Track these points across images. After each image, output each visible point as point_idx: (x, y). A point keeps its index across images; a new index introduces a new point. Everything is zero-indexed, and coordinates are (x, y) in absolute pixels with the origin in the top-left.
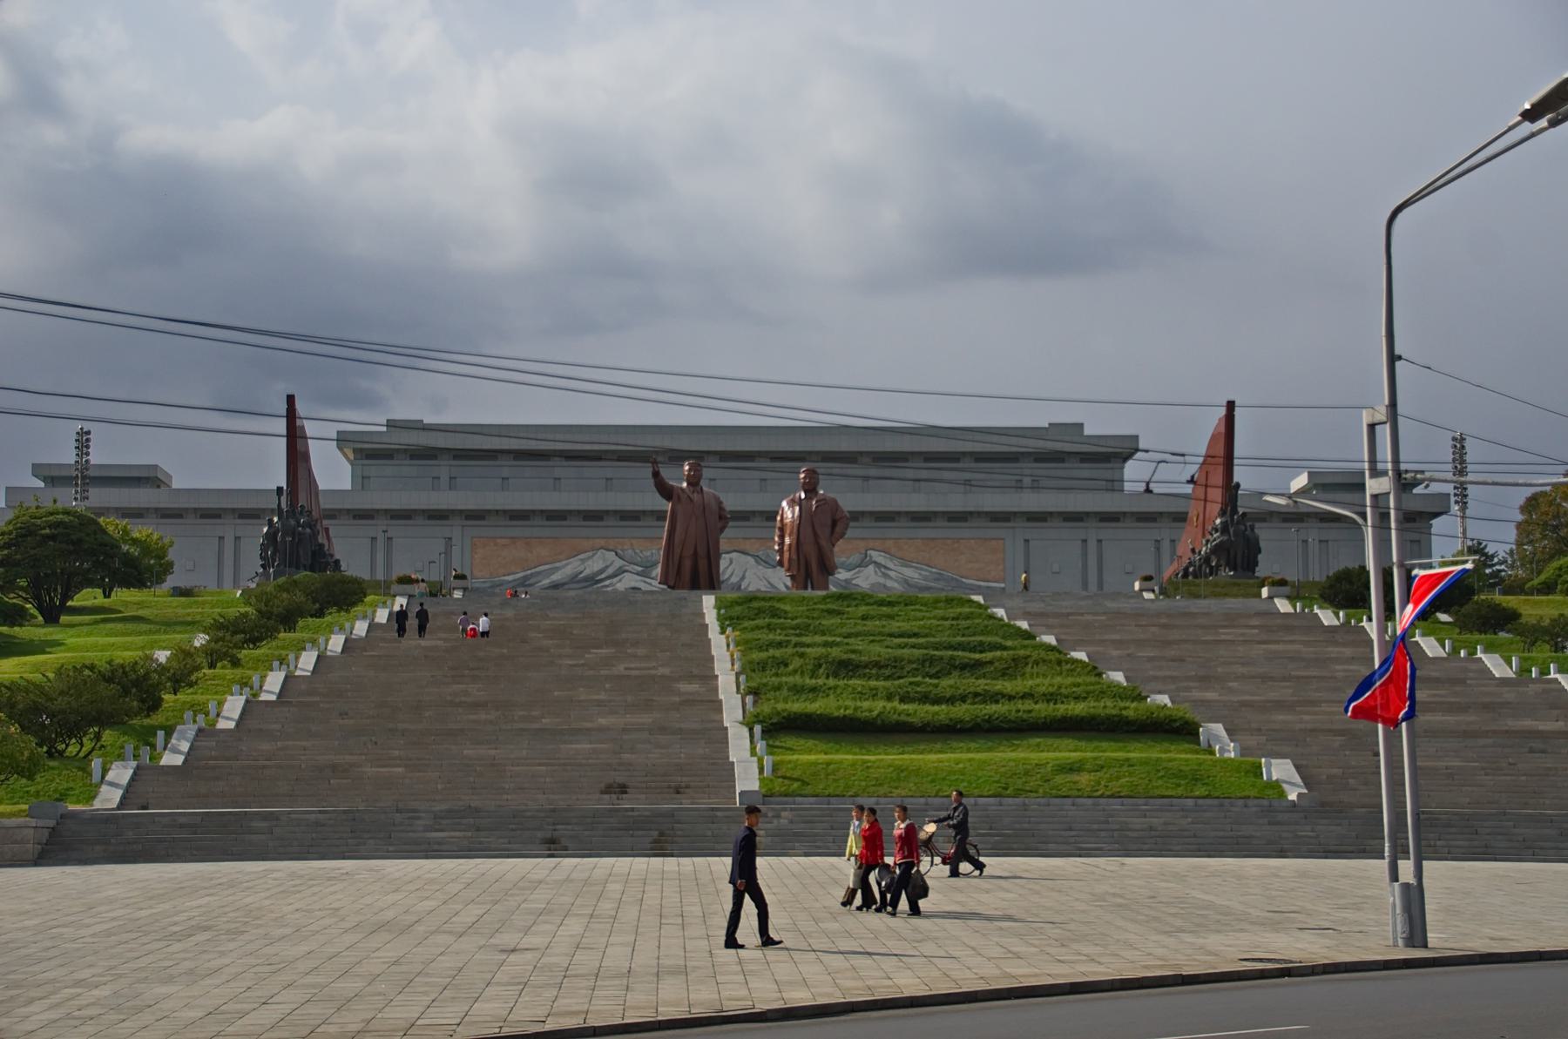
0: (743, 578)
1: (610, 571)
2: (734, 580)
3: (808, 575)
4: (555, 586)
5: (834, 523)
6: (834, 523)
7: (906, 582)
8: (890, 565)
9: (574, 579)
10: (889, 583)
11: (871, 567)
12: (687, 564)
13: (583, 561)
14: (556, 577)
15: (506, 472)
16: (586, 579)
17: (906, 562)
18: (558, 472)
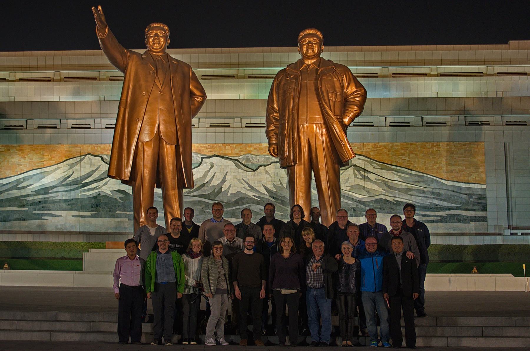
1: (96, 175)
4: (46, 190)
8: (370, 169)
10: (369, 186)
11: (351, 170)
14: (48, 181)
16: (75, 182)
17: (384, 165)
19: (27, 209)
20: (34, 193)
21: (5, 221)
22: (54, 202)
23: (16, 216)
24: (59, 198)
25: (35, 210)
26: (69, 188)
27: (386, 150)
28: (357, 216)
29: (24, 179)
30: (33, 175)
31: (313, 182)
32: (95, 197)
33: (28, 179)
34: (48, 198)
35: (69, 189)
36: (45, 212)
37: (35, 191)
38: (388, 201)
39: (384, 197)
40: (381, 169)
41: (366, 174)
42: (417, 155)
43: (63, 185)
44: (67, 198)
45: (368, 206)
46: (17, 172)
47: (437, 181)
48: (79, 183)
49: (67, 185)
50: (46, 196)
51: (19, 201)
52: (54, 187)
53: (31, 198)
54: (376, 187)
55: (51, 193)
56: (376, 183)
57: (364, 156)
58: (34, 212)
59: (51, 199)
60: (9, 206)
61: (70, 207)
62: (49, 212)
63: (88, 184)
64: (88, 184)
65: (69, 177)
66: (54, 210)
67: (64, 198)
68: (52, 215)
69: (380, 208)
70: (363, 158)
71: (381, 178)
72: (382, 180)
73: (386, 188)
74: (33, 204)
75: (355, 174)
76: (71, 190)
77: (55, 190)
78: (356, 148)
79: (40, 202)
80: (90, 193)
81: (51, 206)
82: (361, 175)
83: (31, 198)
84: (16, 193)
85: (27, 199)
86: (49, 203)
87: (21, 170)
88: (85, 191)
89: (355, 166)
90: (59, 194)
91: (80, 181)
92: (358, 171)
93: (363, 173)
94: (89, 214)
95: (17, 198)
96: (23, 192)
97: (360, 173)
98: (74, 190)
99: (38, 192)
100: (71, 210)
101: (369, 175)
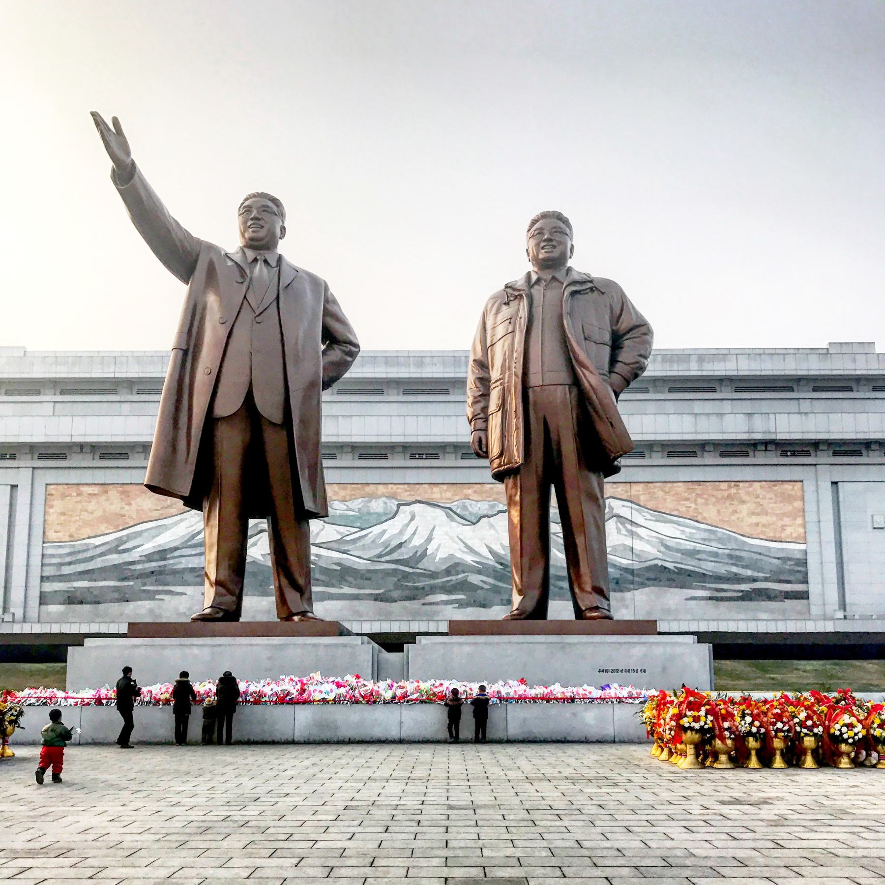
0: (429, 540)
2: (417, 541)
4: (162, 554)
10: (639, 546)
14: (165, 539)
19: (132, 583)
20: (143, 558)
21: (98, 603)
22: (175, 572)
23: (116, 595)
24: (182, 566)
25: (145, 585)
27: (660, 494)
28: (622, 591)
29: (129, 538)
31: (554, 510)
33: (135, 538)
34: (165, 566)
35: (198, 552)
36: (161, 588)
37: (145, 556)
38: (666, 568)
39: (660, 563)
40: (656, 521)
41: (634, 529)
42: (707, 500)
44: (195, 566)
45: (638, 576)
46: (118, 526)
47: (736, 539)
49: (195, 546)
50: (162, 563)
51: (121, 571)
52: (176, 549)
53: (139, 567)
55: (169, 559)
56: (648, 542)
57: (631, 502)
58: (144, 588)
59: (171, 567)
60: (105, 580)
61: (198, 579)
62: (167, 588)
66: (174, 585)
67: (190, 566)
69: (655, 579)
70: (629, 504)
71: (657, 535)
72: (657, 538)
73: (663, 549)
75: (617, 528)
77: (177, 553)
78: (620, 490)
79: (152, 572)
81: (169, 578)
82: (627, 530)
83: (139, 567)
84: (115, 559)
86: (167, 574)
87: (126, 523)
89: (618, 516)
90: (183, 560)
92: (623, 524)
93: (629, 527)
95: (115, 566)
97: (625, 527)
99: (149, 558)
101: (639, 530)
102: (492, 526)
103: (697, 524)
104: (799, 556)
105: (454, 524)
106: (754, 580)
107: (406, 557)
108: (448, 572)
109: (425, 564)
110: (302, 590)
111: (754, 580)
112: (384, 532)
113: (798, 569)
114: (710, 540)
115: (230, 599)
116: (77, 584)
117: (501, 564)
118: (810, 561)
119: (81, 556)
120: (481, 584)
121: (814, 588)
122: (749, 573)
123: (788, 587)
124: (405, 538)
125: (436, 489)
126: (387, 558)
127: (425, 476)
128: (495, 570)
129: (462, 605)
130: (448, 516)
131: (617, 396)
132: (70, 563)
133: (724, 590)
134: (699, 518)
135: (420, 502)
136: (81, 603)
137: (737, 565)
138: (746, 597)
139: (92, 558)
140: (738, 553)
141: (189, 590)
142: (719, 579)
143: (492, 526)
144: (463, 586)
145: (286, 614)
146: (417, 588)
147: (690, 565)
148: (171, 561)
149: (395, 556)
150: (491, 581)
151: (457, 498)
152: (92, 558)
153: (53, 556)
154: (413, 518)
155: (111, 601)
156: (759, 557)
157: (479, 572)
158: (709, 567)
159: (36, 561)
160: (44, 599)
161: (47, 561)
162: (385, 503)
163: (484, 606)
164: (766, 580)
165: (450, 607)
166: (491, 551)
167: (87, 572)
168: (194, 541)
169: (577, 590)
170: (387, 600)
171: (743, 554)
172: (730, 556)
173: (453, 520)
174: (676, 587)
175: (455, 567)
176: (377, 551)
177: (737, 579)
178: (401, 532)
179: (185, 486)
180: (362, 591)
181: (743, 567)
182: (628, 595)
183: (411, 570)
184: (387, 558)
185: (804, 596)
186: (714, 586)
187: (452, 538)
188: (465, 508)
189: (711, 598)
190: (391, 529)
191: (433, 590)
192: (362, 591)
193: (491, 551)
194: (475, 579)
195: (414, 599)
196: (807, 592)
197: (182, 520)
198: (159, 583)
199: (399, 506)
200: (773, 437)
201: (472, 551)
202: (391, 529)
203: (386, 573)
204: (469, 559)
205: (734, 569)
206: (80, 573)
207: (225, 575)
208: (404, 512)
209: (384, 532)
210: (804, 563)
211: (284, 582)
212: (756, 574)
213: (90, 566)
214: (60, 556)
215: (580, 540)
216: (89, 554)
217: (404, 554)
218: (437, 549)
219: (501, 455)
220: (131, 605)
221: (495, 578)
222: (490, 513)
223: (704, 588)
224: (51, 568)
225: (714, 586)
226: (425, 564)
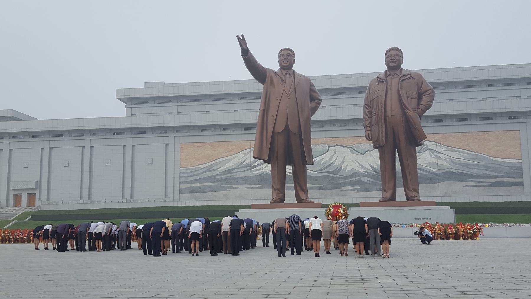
0: (343, 162)
2: (338, 163)
3: (396, 146)
4: (229, 171)
5: (420, 97)
6: (420, 97)
7: (452, 161)
8: (441, 151)
9: (239, 166)
10: (440, 162)
12: (280, 141)
13: (245, 155)
14: (229, 165)
15: (208, 108)
16: (247, 166)
17: (450, 147)
18: (236, 107)
21: (203, 192)
22: (234, 179)
24: (237, 176)
26: (244, 169)
27: (451, 138)
30: (220, 162)
32: (260, 175)
39: (451, 170)
43: (241, 168)
48: (251, 167)
49: (241, 168)
51: (212, 179)
52: (234, 169)
53: (219, 177)
54: (445, 163)
56: (445, 160)
61: (244, 182)
62: (231, 186)
63: (256, 166)
64: (256, 166)
65: (244, 162)
68: (233, 188)
73: (452, 163)
74: (220, 181)
75: (430, 154)
76: (245, 171)
77: (235, 171)
80: (257, 172)
83: (219, 177)
84: (210, 174)
85: (217, 177)
88: (254, 171)
89: (430, 149)
91: (250, 165)
92: (433, 153)
93: (436, 154)
94: (257, 186)
95: (210, 177)
96: (214, 173)
98: (247, 170)
99: (223, 173)
100: (245, 184)
101: (440, 155)
102: (371, 155)
103: (468, 152)
104: (518, 165)
105: (354, 155)
106: (497, 177)
107: (333, 170)
108: (352, 176)
109: (341, 173)
110: (305, 191)
111: (497, 177)
112: (323, 159)
113: (518, 171)
114: (475, 159)
115: (281, 195)
116: (194, 185)
117: (376, 172)
118: (523, 167)
119: (195, 173)
120: (367, 182)
121: (526, 180)
122: (494, 174)
123: (513, 180)
124: (332, 162)
125: (345, 139)
126: (324, 171)
127: (341, 134)
128: (373, 175)
129: (358, 191)
130: (351, 151)
131: (420, 117)
132: (191, 176)
133: (482, 182)
134: (469, 149)
135: (338, 145)
136: (196, 193)
137: (488, 170)
138: (493, 185)
139: (200, 174)
140: (488, 165)
141: (240, 186)
142: (479, 177)
143: (371, 155)
144: (359, 182)
145: (299, 200)
146: (338, 184)
147: (466, 171)
148: (232, 174)
149: (328, 170)
150: (371, 180)
151: (355, 143)
152: (200, 174)
153: (183, 173)
154: (335, 153)
155: (209, 192)
156: (498, 166)
157: (366, 176)
158: (475, 171)
159: (177, 176)
160: (181, 191)
161: (182, 175)
162: (323, 146)
163: (368, 191)
164: (502, 177)
165: (353, 192)
166: (372, 167)
167: (198, 179)
168: (241, 166)
169: (407, 190)
170: (325, 190)
171: (490, 165)
172: (485, 167)
173: (354, 153)
174: (459, 181)
175: (355, 174)
176: (320, 168)
177: (488, 177)
178: (331, 159)
179: (266, 158)
180: (314, 186)
181: (491, 171)
182: (436, 185)
183: (335, 176)
184: (324, 171)
185: (521, 184)
186: (477, 180)
187: (353, 161)
188: (359, 147)
189: (475, 186)
190: (326, 158)
191: (345, 184)
192: (314, 186)
193: (372, 167)
194: (364, 179)
195: (336, 188)
196: (523, 182)
197: (236, 157)
198: (227, 183)
199: (329, 147)
200: (504, 111)
201: (362, 167)
202: (326, 158)
203: (324, 177)
204: (361, 170)
205: (487, 172)
206: (196, 180)
207: (279, 187)
208: (331, 150)
209: (323, 159)
210: (521, 169)
211: (298, 188)
212: (497, 174)
213: (199, 177)
214: (187, 173)
215: (407, 171)
216: (199, 172)
217: (331, 169)
218: (347, 166)
219: (377, 141)
220: (216, 193)
221: (373, 179)
222: (370, 150)
223: (472, 181)
224: (184, 178)
225: (477, 180)
226: (341, 173)
